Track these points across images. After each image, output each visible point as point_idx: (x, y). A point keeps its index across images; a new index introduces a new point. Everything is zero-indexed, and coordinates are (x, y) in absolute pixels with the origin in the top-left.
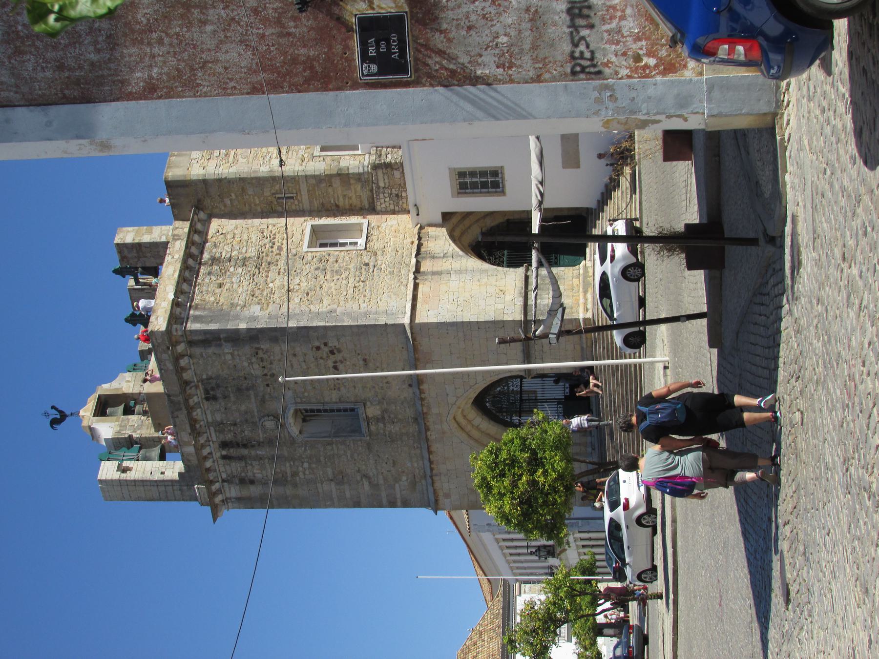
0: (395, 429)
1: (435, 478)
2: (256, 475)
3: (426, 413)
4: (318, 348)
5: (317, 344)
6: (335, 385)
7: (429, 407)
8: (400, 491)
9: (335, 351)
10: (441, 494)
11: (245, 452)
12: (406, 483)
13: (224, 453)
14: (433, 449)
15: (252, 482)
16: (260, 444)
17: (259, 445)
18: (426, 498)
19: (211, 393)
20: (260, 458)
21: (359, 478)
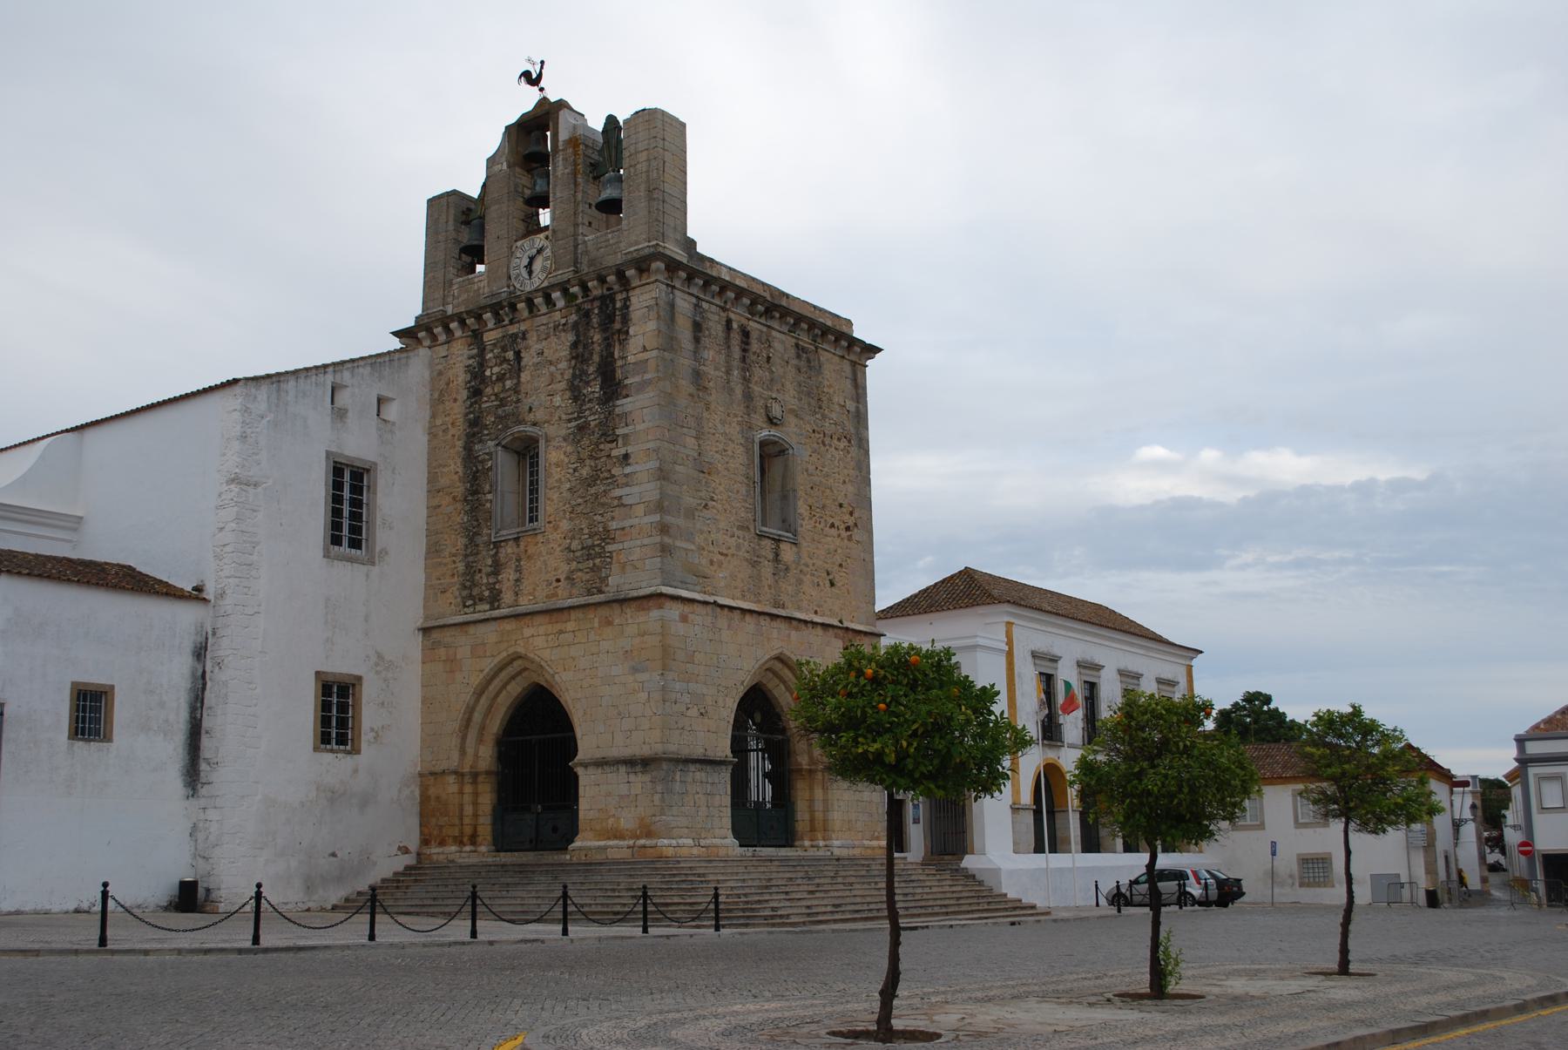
0: (767, 569)
1: (709, 608)
2: (706, 351)
3: (791, 623)
4: (851, 514)
5: (856, 515)
6: (814, 516)
7: (797, 629)
8: (686, 549)
9: (849, 533)
10: (687, 609)
11: (737, 352)
12: (697, 561)
13: (735, 326)
14: (748, 617)
15: (697, 340)
16: (746, 381)
17: (744, 378)
18: (674, 584)
19: (805, 355)
20: (728, 372)
21: (702, 494)
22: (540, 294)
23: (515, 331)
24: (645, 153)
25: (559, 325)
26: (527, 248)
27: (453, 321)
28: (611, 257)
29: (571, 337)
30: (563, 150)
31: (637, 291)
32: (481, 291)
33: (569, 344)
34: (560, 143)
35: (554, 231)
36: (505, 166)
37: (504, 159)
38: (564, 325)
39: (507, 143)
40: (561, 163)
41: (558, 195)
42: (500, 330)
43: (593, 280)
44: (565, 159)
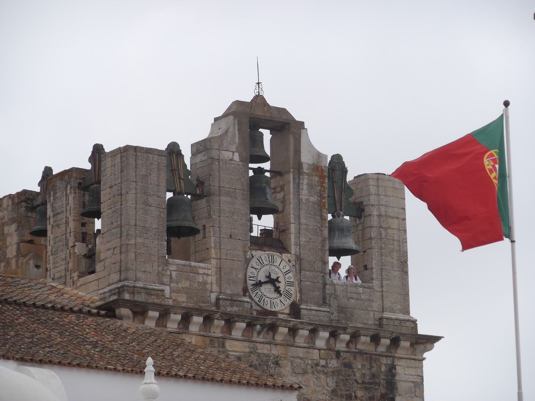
22: (310, 327)
23: (266, 352)
24: (396, 221)
25: (317, 365)
26: (265, 263)
27: (199, 315)
28: (363, 312)
29: (331, 383)
30: (307, 174)
31: (402, 363)
32: (208, 287)
33: (329, 389)
34: (305, 169)
35: (299, 258)
36: (236, 157)
37: (233, 148)
38: (323, 366)
39: (237, 132)
40: (305, 187)
41: (303, 221)
42: (246, 344)
43: (367, 336)
44: (311, 186)
